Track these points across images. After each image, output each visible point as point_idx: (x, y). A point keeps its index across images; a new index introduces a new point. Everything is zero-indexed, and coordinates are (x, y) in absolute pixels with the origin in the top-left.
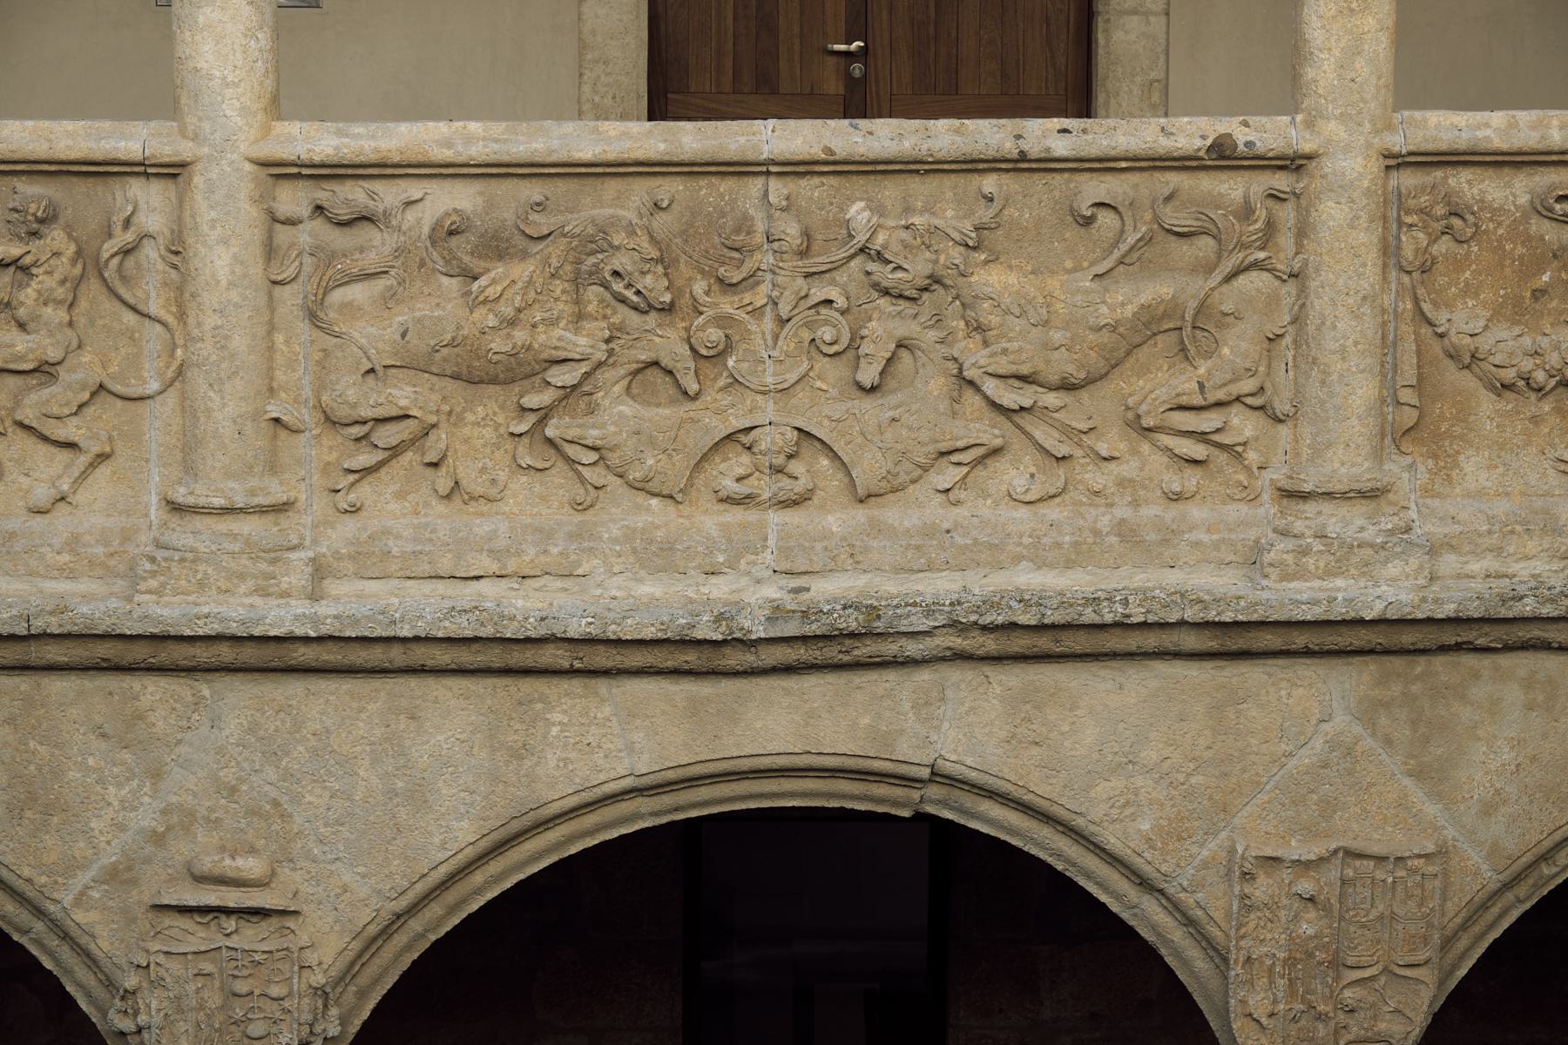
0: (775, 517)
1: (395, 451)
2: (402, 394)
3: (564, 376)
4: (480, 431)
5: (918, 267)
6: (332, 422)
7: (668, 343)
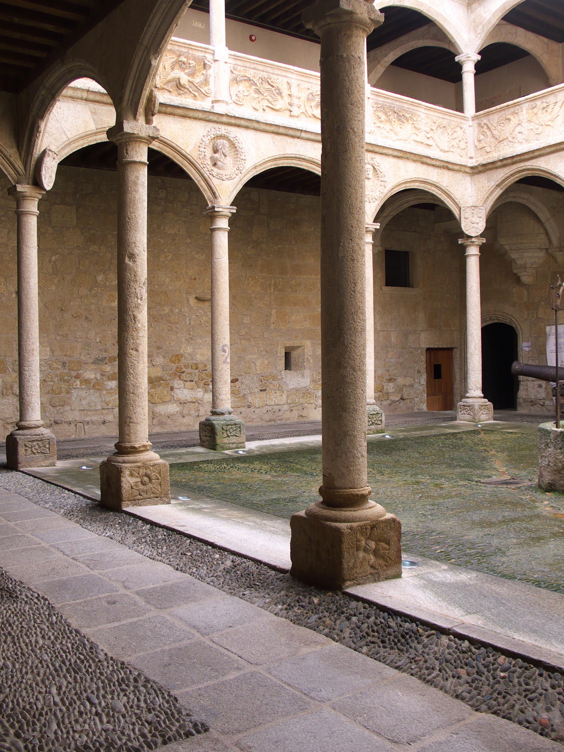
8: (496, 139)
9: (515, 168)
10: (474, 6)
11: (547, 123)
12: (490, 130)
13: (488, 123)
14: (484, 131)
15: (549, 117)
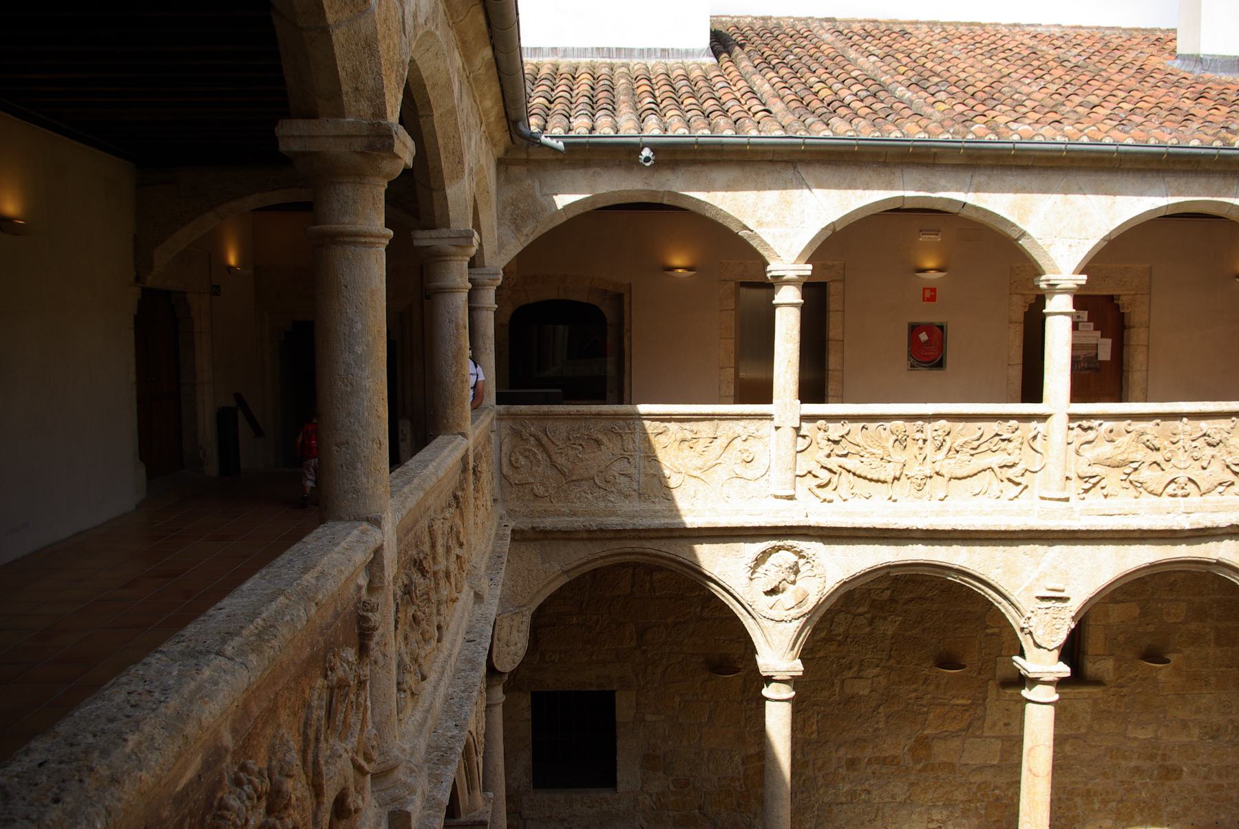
0: (1180, 499)
1: (1094, 485)
2: (1097, 470)
3: (1135, 465)
4: (1113, 478)
5: (1217, 438)
6: (1081, 478)
7: (1157, 456)
8: (563, 474)
9: (615, 546)
10: (516, 171)
11: (694, 473)
12: (545, 450)
13: (541, 435)
14: (526, 450)
15: (700, 463)
